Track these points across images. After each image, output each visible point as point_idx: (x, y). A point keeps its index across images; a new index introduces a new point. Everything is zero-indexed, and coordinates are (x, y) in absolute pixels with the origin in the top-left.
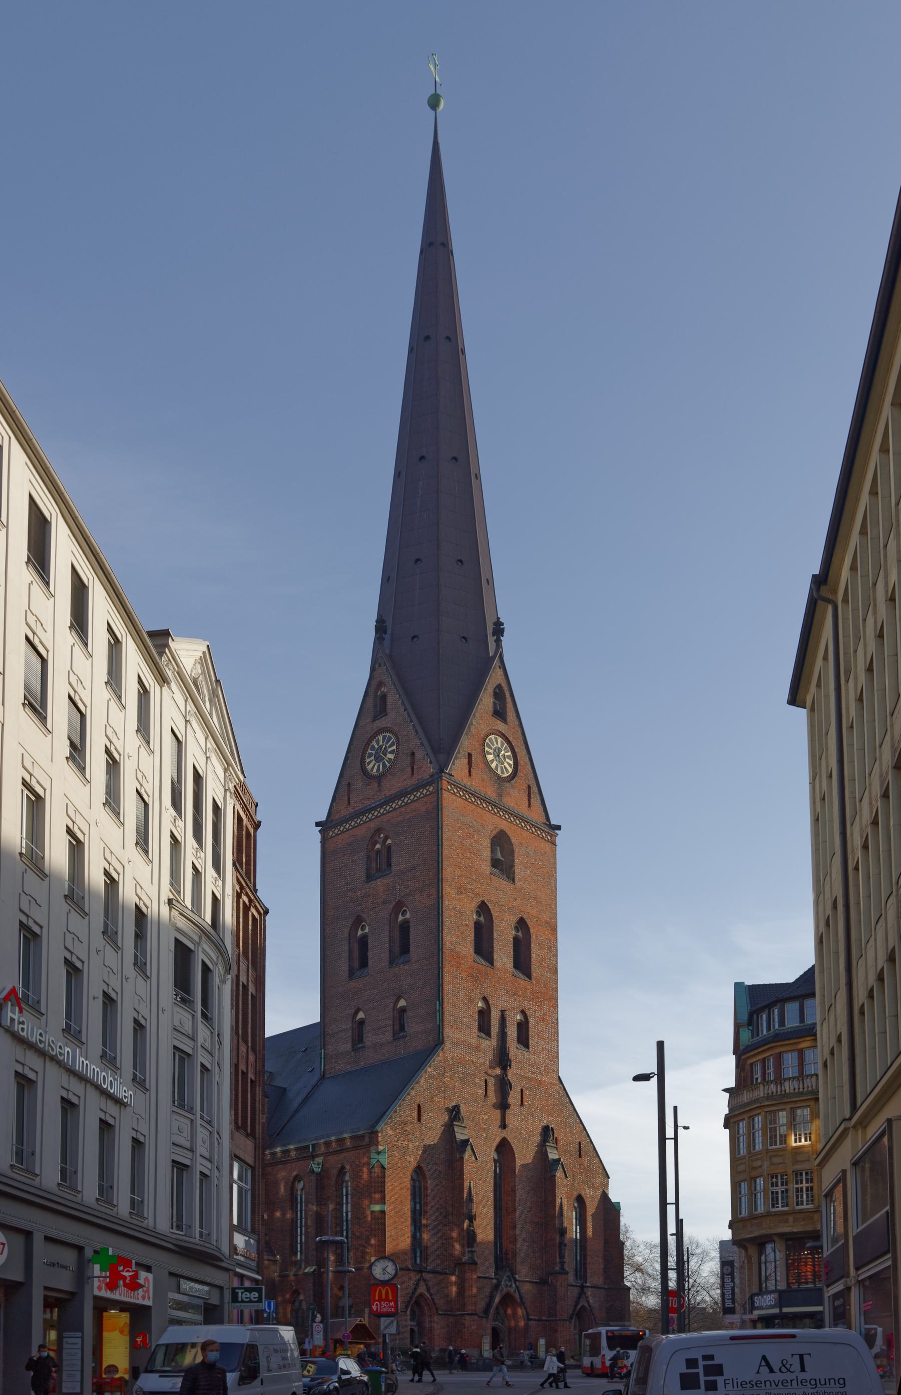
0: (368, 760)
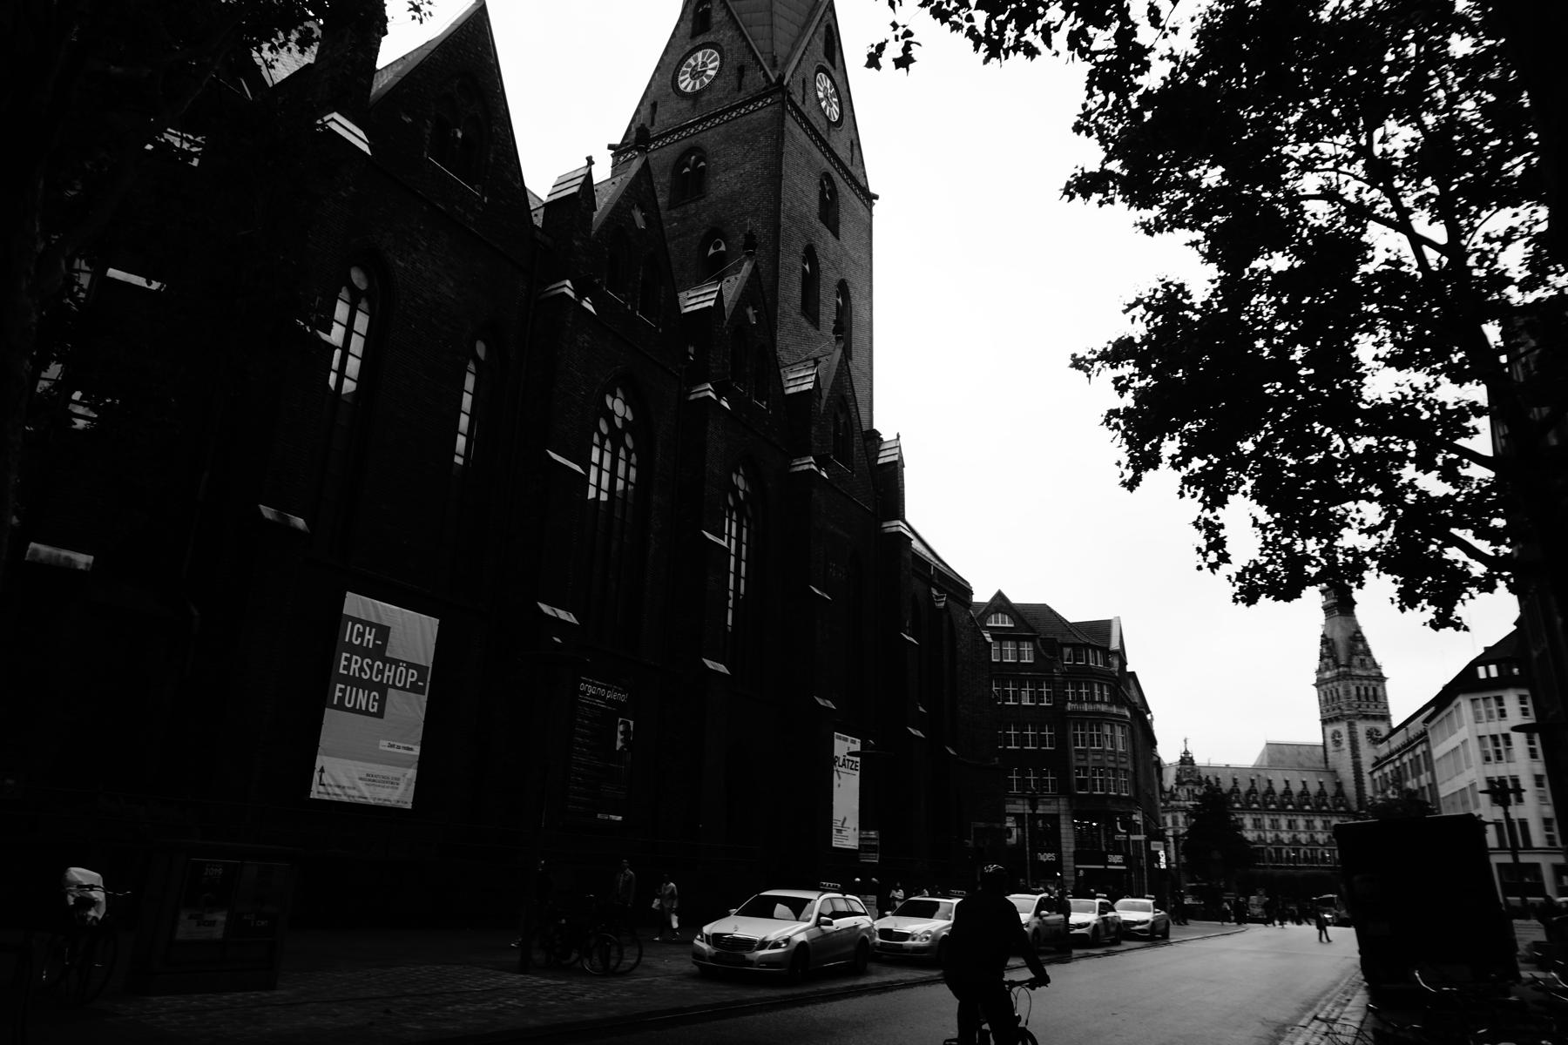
0: (681, 78)
